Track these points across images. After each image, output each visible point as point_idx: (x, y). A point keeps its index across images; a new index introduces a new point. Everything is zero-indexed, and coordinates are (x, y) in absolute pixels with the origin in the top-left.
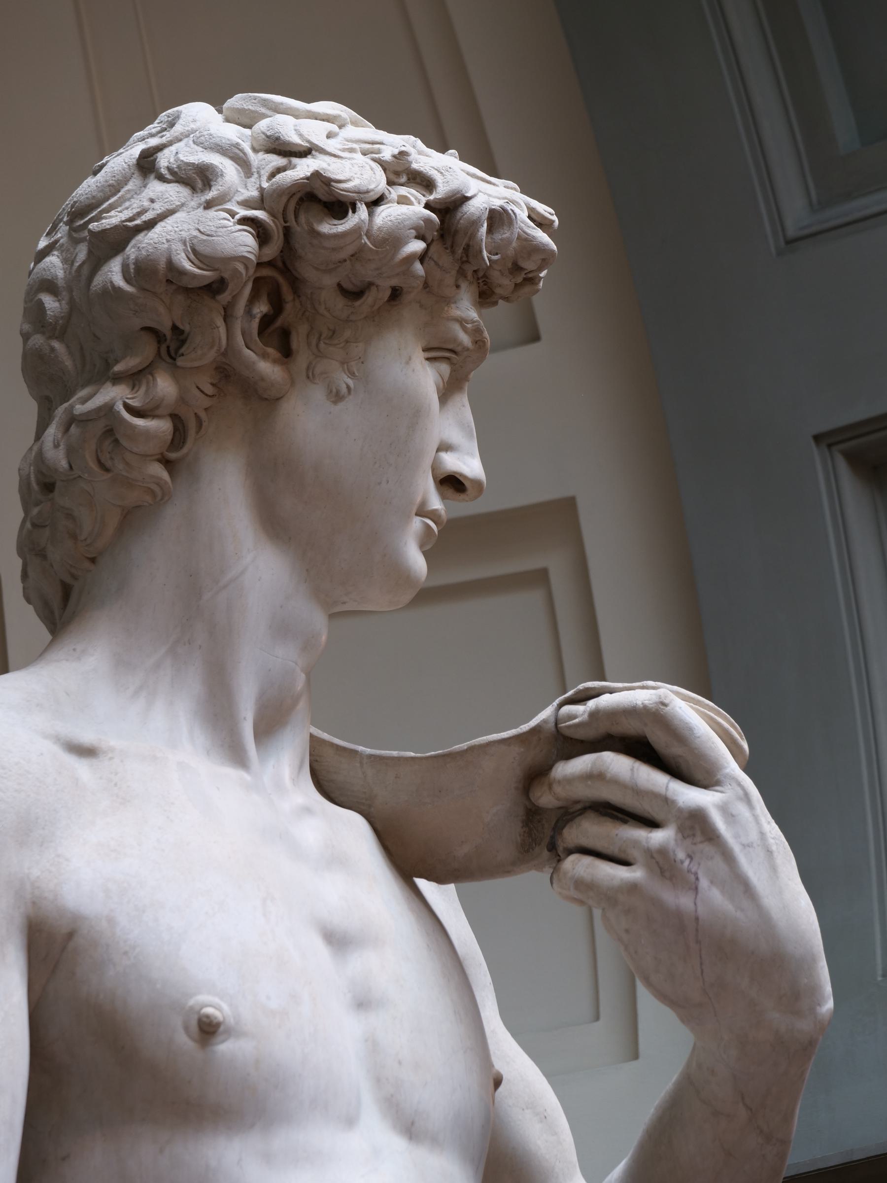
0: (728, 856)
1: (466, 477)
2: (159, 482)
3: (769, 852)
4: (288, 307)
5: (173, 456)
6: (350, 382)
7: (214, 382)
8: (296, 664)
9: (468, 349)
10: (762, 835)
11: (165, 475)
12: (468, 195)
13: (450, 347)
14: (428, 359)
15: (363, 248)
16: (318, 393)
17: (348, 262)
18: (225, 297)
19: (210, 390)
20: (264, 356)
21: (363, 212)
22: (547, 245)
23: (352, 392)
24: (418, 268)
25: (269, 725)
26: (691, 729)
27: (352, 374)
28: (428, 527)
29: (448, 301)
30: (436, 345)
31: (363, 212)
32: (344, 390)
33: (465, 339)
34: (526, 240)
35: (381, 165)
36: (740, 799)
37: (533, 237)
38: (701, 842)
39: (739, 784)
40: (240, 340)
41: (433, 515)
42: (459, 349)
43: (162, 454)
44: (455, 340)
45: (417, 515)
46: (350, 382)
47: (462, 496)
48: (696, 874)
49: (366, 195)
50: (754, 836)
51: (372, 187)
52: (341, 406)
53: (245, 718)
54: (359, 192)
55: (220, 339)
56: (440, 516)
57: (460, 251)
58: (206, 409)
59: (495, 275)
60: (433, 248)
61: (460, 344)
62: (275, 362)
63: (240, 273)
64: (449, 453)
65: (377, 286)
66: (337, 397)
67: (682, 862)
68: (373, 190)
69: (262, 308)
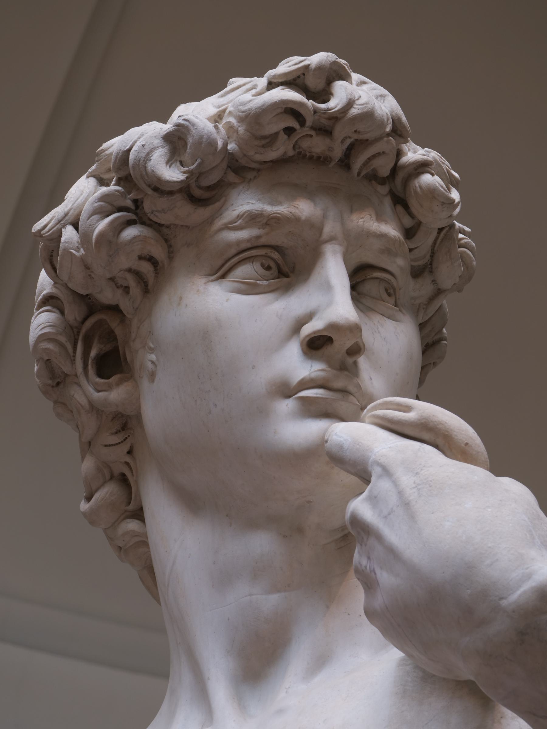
0: (379, 537)
1: (319, 331)
2: (135, 534)
3: (406, 505)
4: (118, 331)
5: (131, 507)
6: (153, 357)
7: (114, 431)
8: (251, 595)
9: (258, 237)
10: (400, 493)
11: (132, 525)
12: (128, 147)
13: (233, 251)
14: (223, 277)
15: (82, 259)
16: (145, 384)
17: (93, 275)
18: (67, 369)
19: (115, 439)
20: (109, 388)
21: (69, 234)
22: (263, 105)
23: (157, 363)
24: (130, 232)
25: (260, 657)
26: (341, 447)
27: (152, 350)
28: (302, 399)
29: (210, 221)
30: (220, 262)
31: (69, 234)
32: (150, 366)
33: (243, 234)
34: (247, 117)
35: (94, 176)
36: (380, 477)
37: (250, 109)
38: (367, 539)
39: (379, 464)
40: (90, 390)
41: (305, 384)
42: (244, 246)
43: (126, 511)
44: (229, 245)
45: (289, 397)
46: (153, 357)
47: (336, 344)
48: (374, 569)
49: (67, 218)
50: (393, 500)
51: (69, 207)
52: (156, 380)
53: (208, 679)
54: (59, 221)
55: (79, 403)
56: (312, 380)
57: (150, 192)
58: (130, 452)
59: (258, 157)
60: (147, 206)
61: (239, 242)
62: (118, 384)
63: (46, 349)
64: (313, 320)
65: (130, 270)
66: (152, 376)
67: (366, 567)
68: (71, 209)
69: (93, 353)
